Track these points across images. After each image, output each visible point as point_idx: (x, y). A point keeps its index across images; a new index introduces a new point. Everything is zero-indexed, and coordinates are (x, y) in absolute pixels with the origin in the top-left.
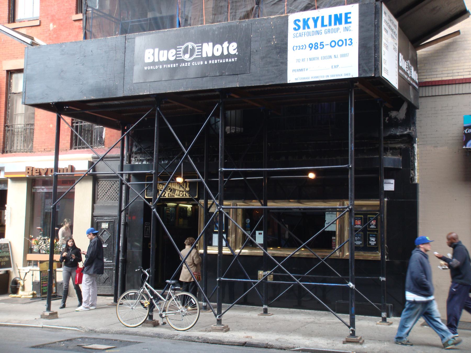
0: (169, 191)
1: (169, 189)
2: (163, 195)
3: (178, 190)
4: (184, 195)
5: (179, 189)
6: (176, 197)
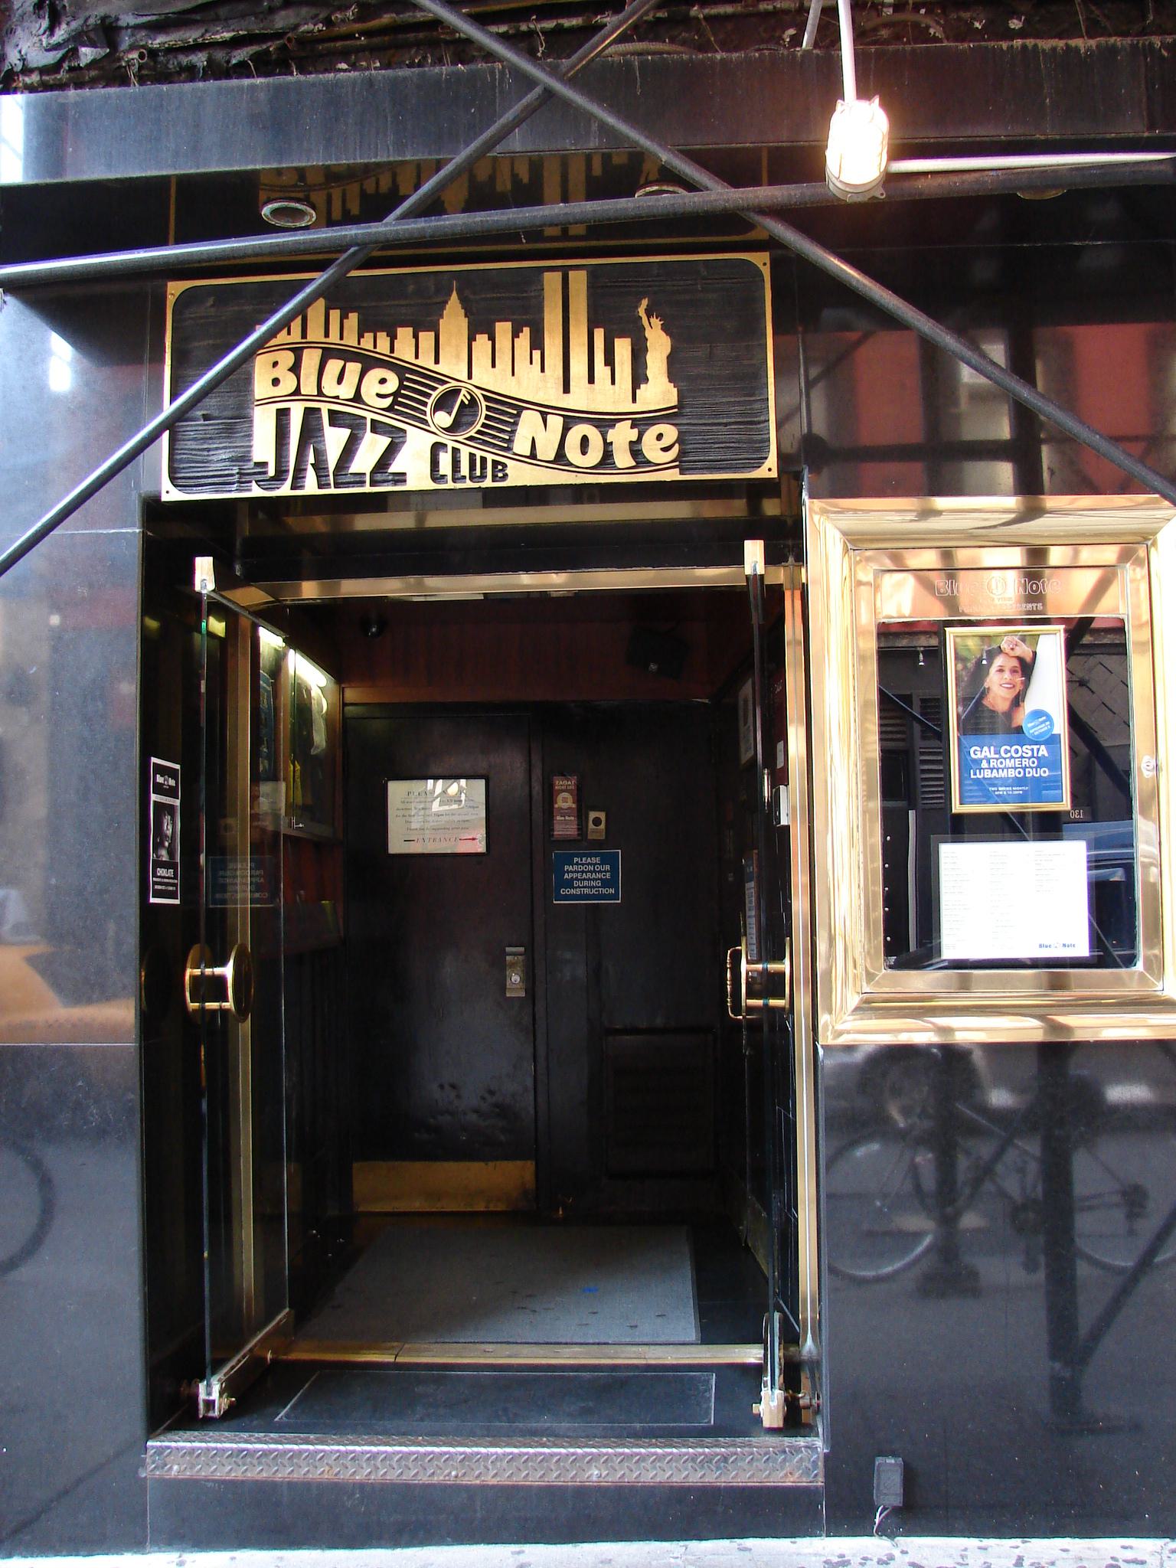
0: (444, 419)
1: (442, 404)
2: (364, 461)
3: (545, 412)
4: (623, 459)
5: (551, 394)
6: (520, 475)
